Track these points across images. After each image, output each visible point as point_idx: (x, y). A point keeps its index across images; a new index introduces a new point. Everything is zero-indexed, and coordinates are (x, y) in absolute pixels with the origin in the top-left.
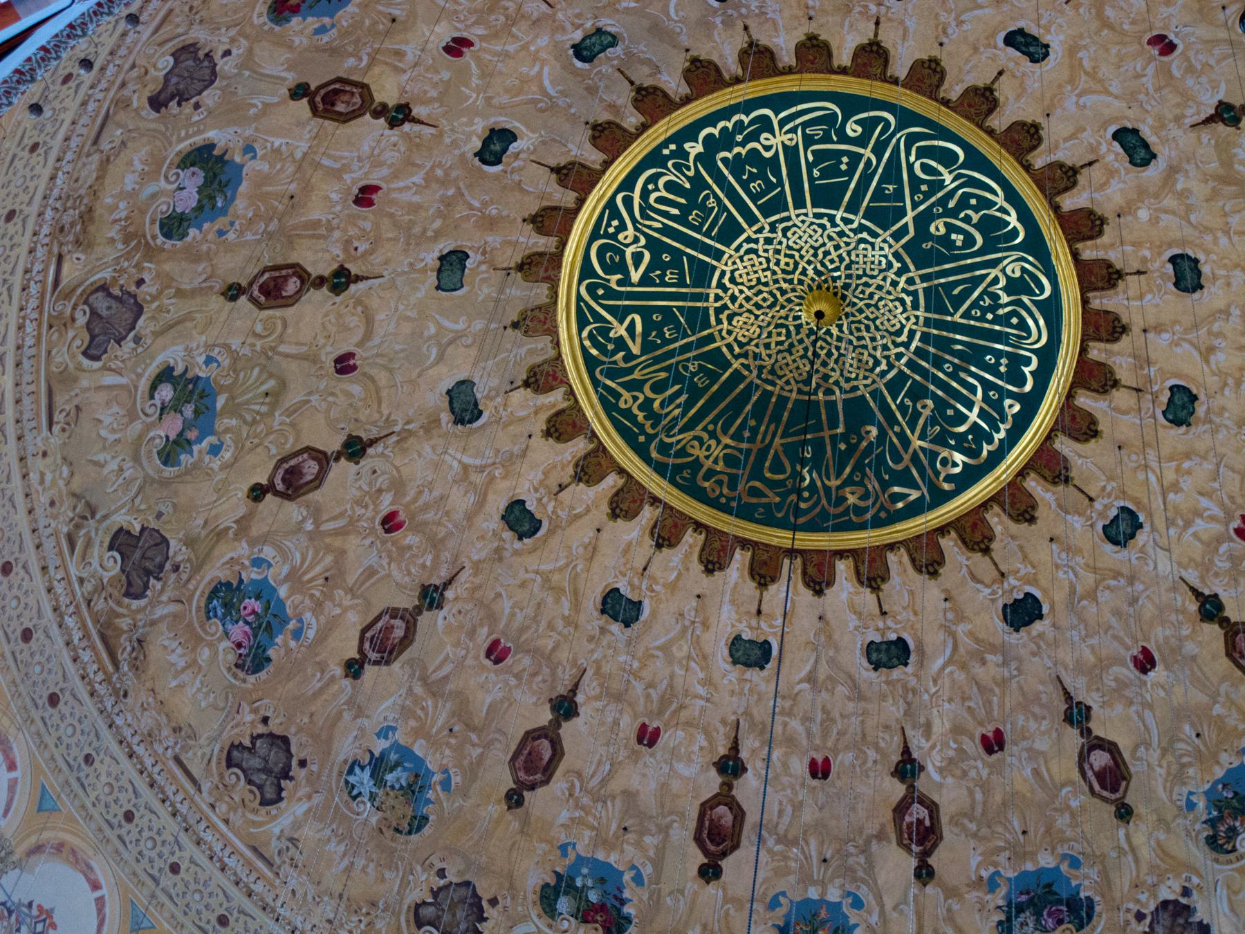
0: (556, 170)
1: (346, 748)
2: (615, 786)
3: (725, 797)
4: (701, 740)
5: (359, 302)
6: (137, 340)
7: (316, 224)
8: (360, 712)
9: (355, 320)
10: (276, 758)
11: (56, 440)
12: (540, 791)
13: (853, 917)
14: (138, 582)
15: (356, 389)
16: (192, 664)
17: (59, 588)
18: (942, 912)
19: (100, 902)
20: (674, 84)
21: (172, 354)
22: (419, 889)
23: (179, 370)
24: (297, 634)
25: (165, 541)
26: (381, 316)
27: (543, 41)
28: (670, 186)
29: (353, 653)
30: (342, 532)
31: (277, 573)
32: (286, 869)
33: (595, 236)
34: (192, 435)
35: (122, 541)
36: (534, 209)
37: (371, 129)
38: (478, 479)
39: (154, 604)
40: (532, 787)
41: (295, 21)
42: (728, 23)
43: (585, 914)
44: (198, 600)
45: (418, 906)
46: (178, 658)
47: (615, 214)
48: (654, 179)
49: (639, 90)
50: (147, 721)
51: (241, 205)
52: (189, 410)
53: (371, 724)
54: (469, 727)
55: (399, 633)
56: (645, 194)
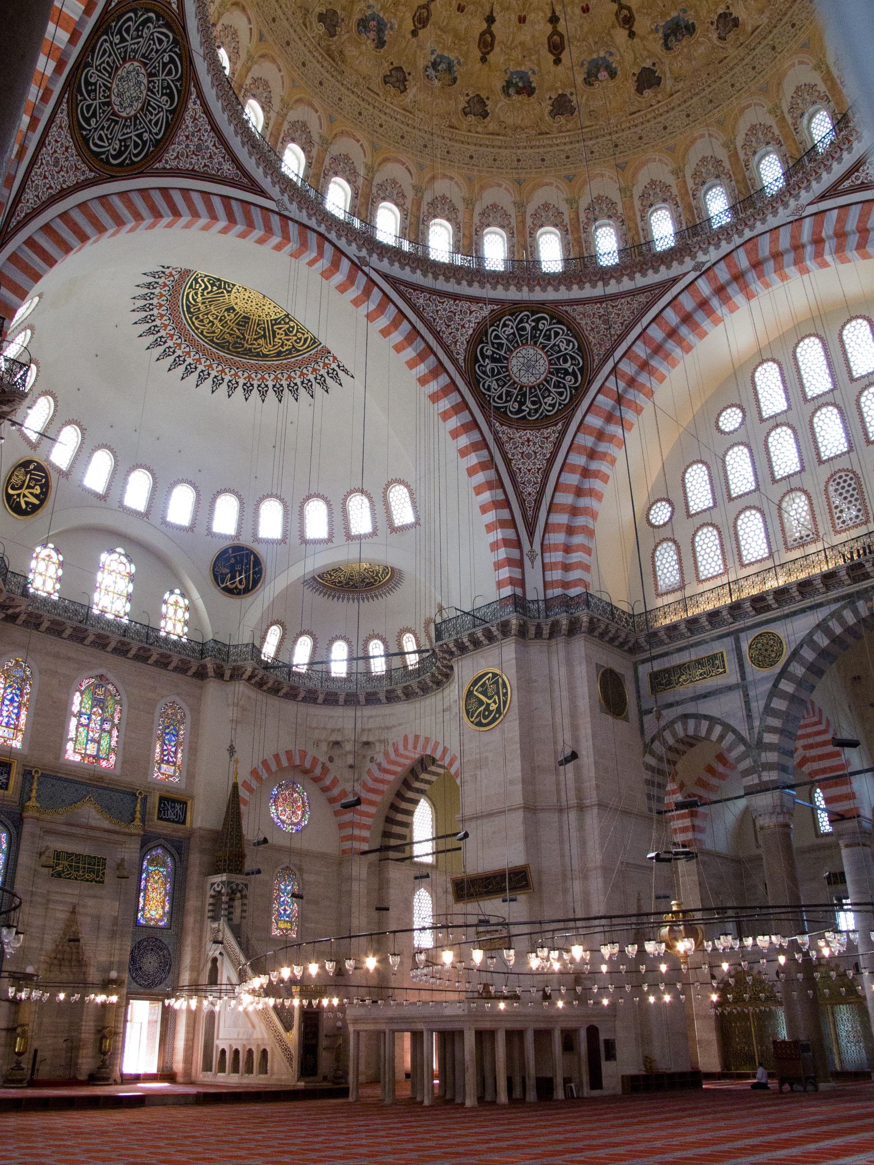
1: (421, 63)
2: (516, 42)
3: (555, 32)
4: (541, 14)
8: (422, 49)
10: (399, 74)
12: (491, 54)
13: (611, 59)
16: (361, 53)
17: (308, 43)
18: (641, 47)
19: (361, 145)
22: (462, 102)
24: (391, 28)
25: (335, 12)
32: (417, 112)
35: (321, 18)
39: (340, 36)
40: (488, 53)
43: (519, 92)
44: (354, 28)
45: (464, 109)
46: (355, 52)
53: (428, 50)
54: (460, 40)
55: (426, 14)
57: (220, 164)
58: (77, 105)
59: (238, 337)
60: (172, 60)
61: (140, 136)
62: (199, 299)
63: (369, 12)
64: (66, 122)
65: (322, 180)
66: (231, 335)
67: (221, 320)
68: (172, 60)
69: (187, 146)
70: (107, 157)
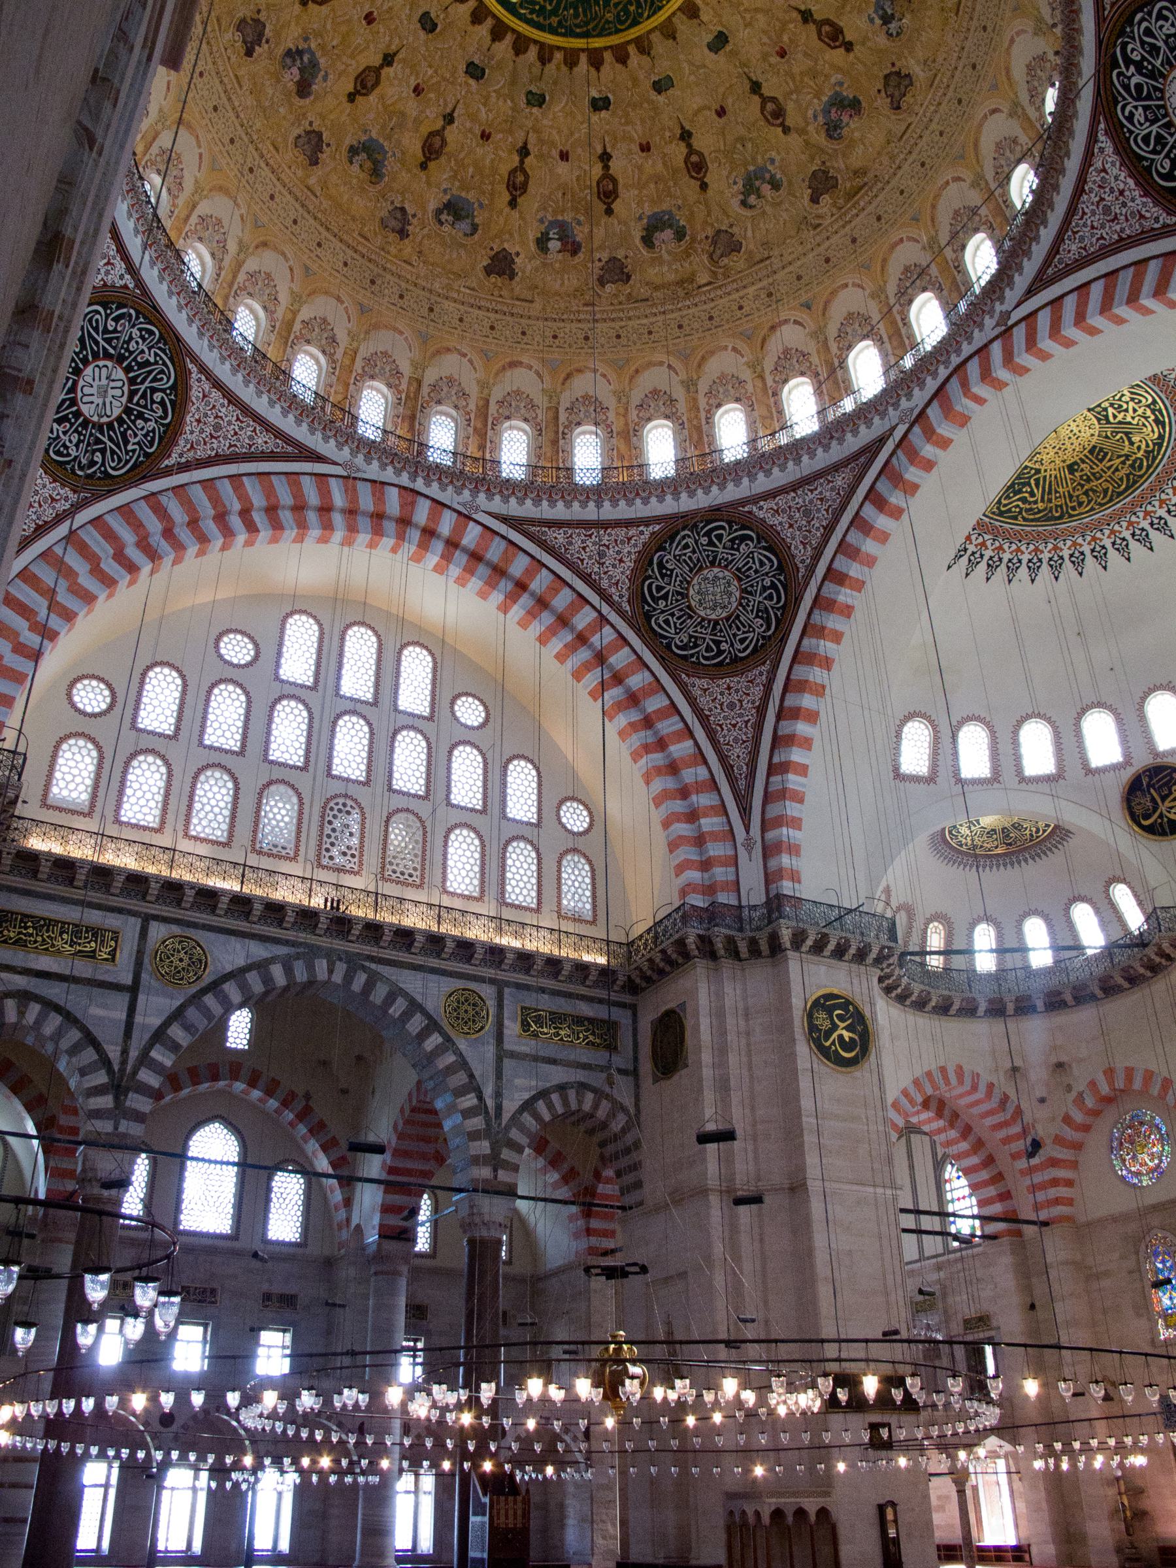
0: (598, 69)
5: (692, 121)
6: (731, 226)
7: (665, 164)
9: (701, 119)
11: (776, 252)
14: (831, 182)
15: (730, 101)
20: (532, 53)
21: (735, 203)
23: (741, 197)
24: (841, 84)
26: (695, 106)
27: (545, 122)
28: (576, 16)
29: (842, 50)
30: (793, 79)
31: (817, 105)
33: (618, 31)
34: (767, 176)
35: (815, 200)
36: (619, 66)
37: (616, 166)
38: (748, 16)
39: (838, 170)
41: (578, 239)
42: (492, 58)
46: (860, 150)
47: (603, 29)
48: (577, 26)
49: (544, 64)
50: (885, 160)
51: (665, 207)
52: (757, 183)
55: (826, 28)
56: (587, 23)
57: (832, 489)
58: (699, 663)
59: (1123, 463)
60: (708, 534)
61: (764, 589)
62: (1040, 505)
63: (821, 120)
64: (704, 683)
65: (959, 278)
66: (1117, 470)
67: (1088, 480)
68: (708, 534)
69: (800, 528)
70: (764, 638)
